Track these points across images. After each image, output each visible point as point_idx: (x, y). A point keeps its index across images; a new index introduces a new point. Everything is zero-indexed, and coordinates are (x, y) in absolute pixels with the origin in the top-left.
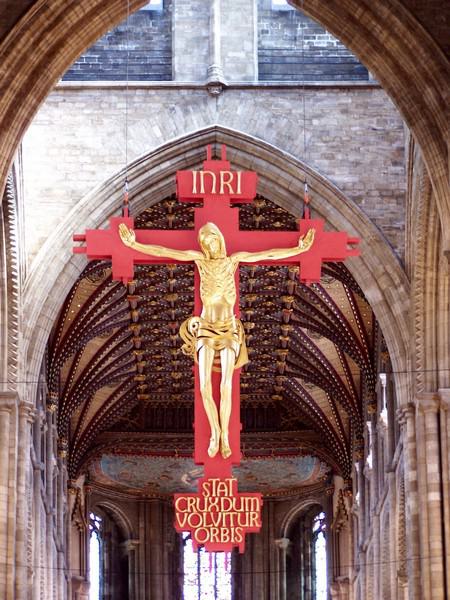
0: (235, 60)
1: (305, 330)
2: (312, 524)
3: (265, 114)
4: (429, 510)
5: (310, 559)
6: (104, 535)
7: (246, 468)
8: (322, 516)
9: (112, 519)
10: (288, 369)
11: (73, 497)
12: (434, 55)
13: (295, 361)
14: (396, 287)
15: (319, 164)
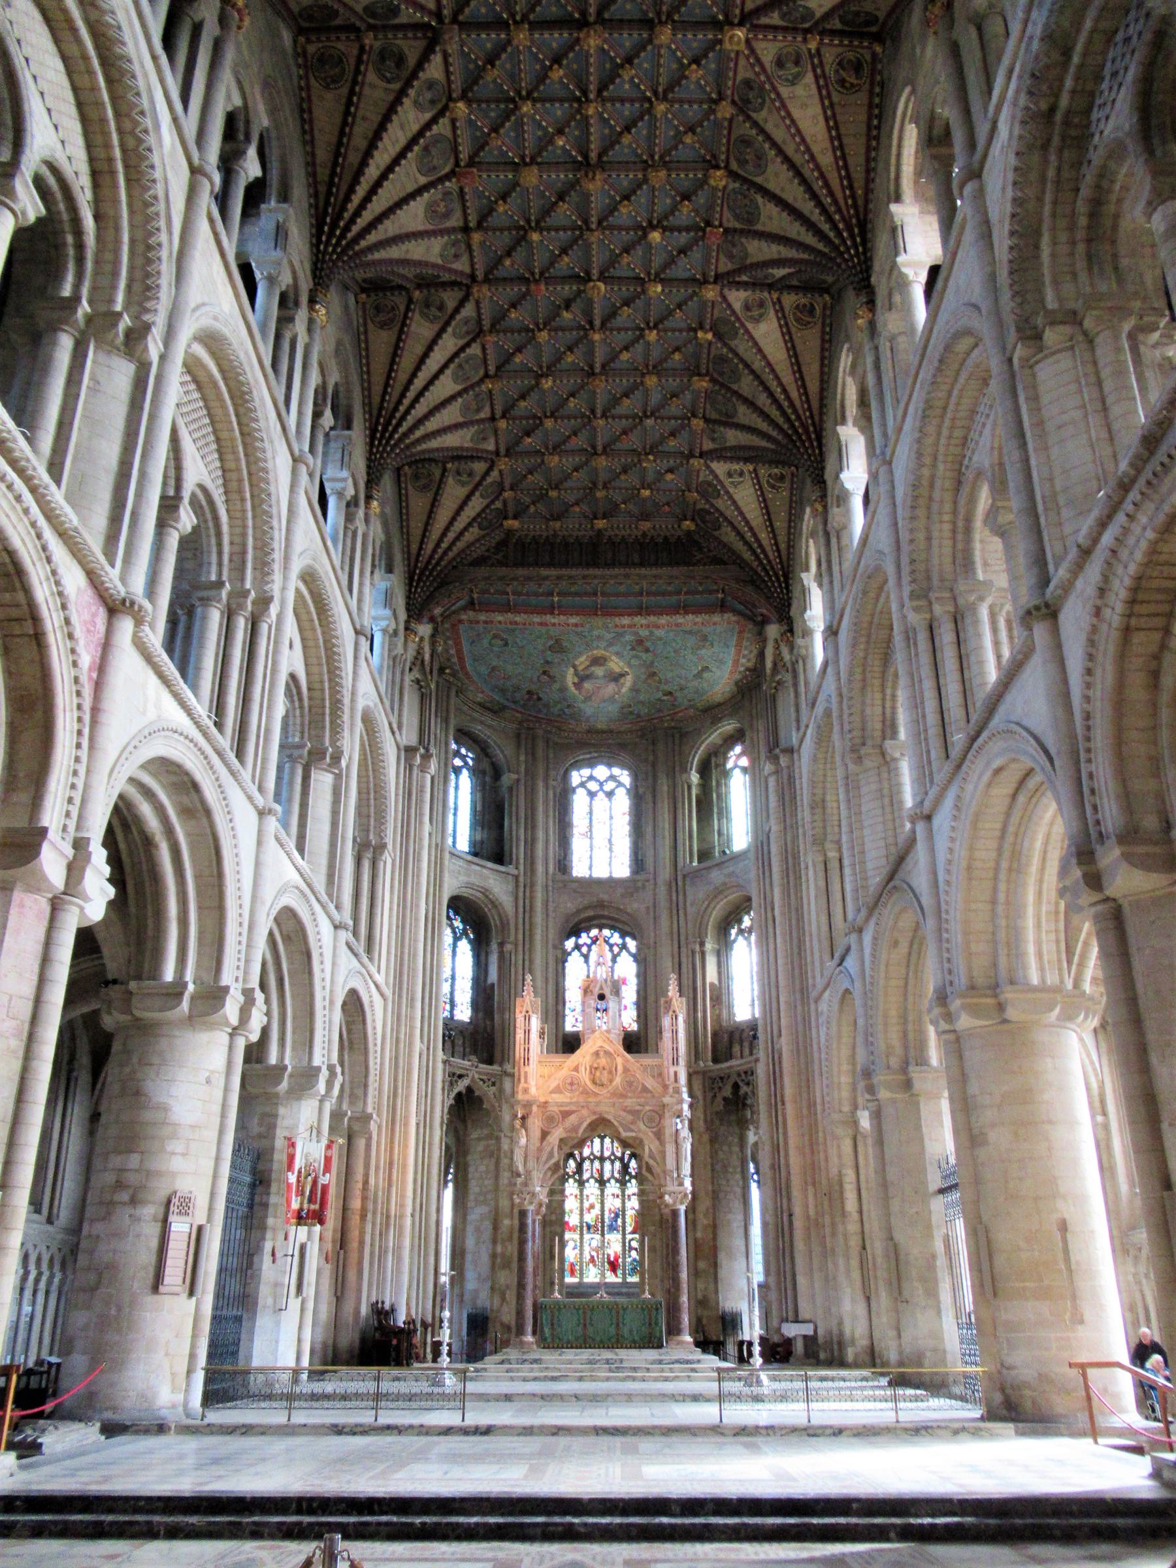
2: (726, 759)
5: (723, 798)
6: (476, 772)
7: (647, 650)
8: (738, 749)
9: (487, 755)
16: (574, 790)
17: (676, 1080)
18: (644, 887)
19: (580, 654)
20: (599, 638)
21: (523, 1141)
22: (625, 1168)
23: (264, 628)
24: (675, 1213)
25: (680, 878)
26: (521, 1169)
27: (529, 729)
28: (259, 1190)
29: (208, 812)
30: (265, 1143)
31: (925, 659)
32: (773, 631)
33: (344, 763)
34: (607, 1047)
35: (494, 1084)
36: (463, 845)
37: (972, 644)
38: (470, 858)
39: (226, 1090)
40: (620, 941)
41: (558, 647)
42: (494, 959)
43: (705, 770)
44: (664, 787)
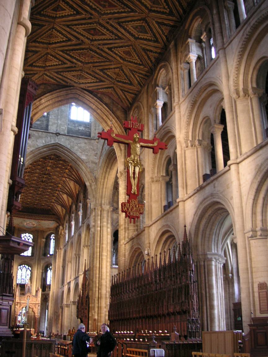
0: (63, 129)
1: (61, 193)
2: (51, 236)
3: (68, 141)
4: (97, 231)
8: (53, 235)
10: (54, 202)
12: (121, 128)
13: (57, 200)
14: (93, 182)
15: (79, 154)
31: (75, 261)
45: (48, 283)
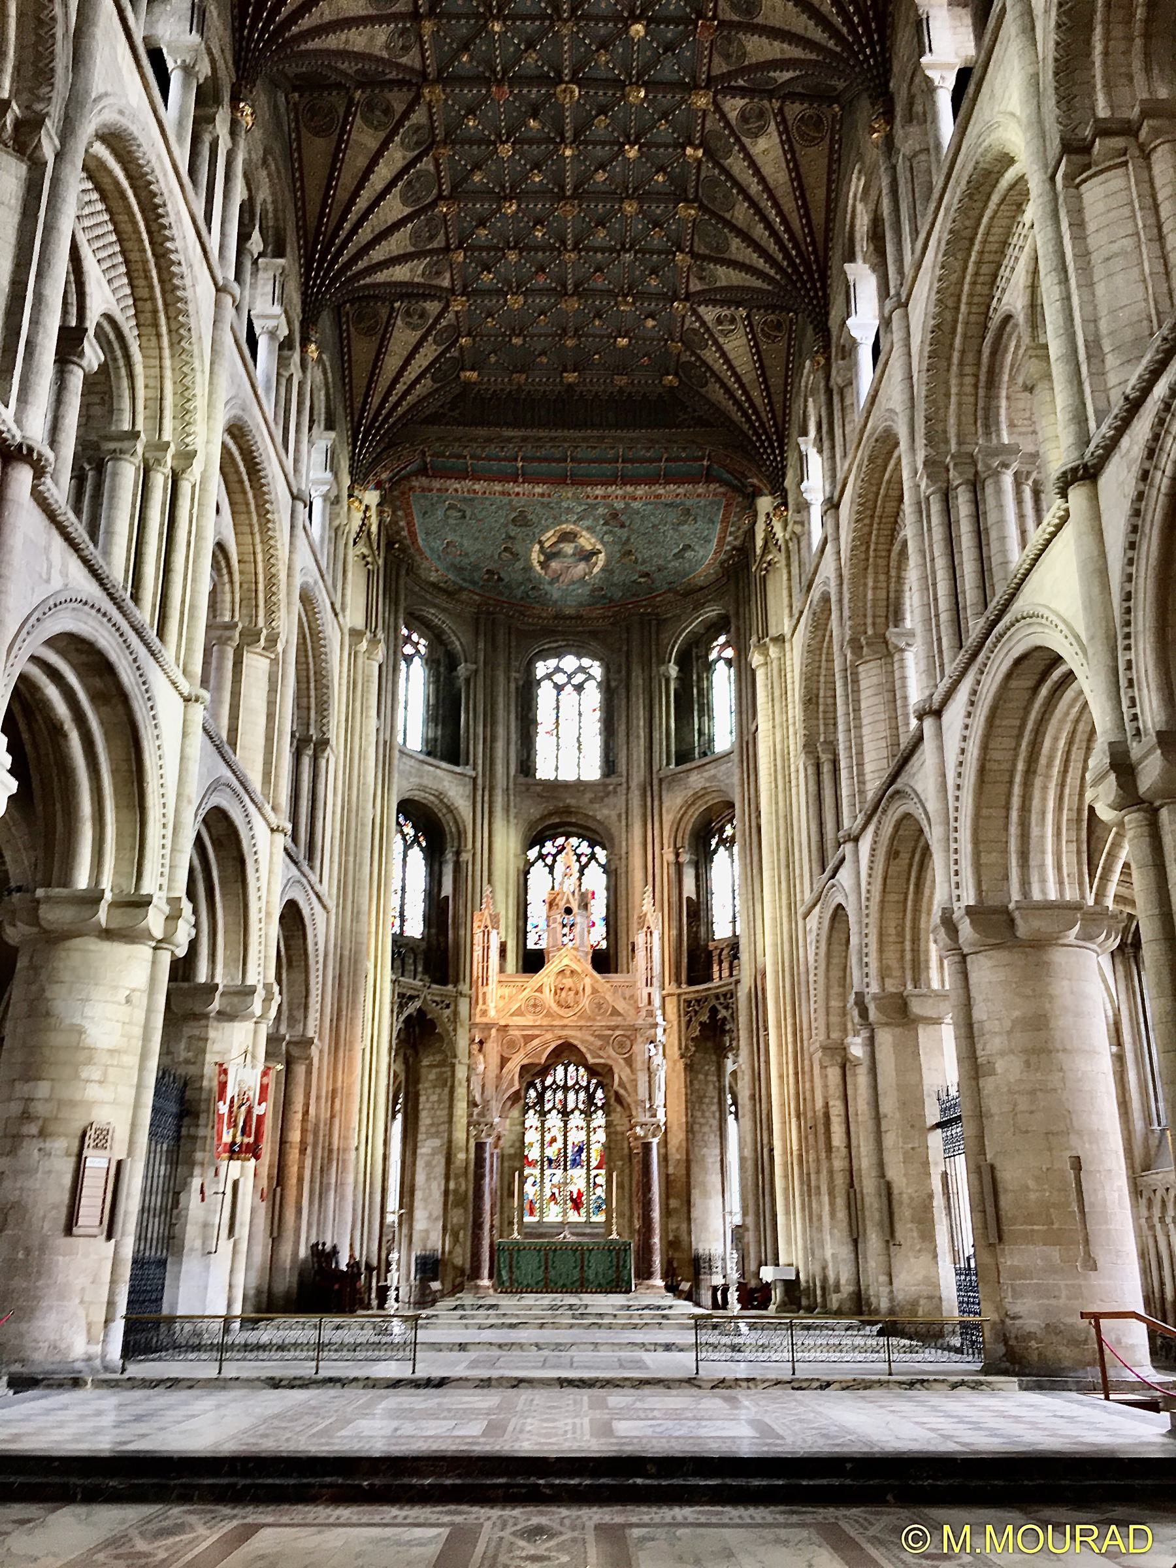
2: (709, 650)
6: (431, 662)
7: (622, 526)
8: (722, 639)
11: (357, 517)
16: (539, 682)
17: (650, 1003)
18: (615, 792)
19: (547, 529)
20: (569, 510)
21: (481, 1068)
22: (591, 1097)
23: (185, 487)
24: (647, 1147)
25: (655, 782)
26: (478, 1099)
27: (489, 613)
28: (186, 1121)
29: (123, 698)
30: (192, 1070)
31: (938, 533)
32: (765, 504)
33: (280, 647)
34: (574, 966)
35: (448, 1006)
36: (415, 743)
37: (992, 517)
38: (422, 757)
39: (149, 1011)
40: (589, 851)
41: (522, 520)
42: (448, 870)
43: (684, 662)
44: (638, 681)
45: (722, 930)
